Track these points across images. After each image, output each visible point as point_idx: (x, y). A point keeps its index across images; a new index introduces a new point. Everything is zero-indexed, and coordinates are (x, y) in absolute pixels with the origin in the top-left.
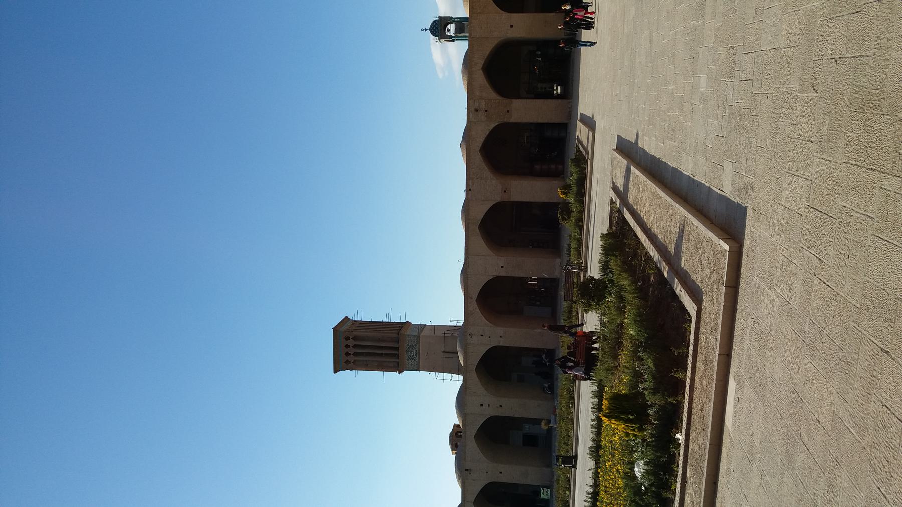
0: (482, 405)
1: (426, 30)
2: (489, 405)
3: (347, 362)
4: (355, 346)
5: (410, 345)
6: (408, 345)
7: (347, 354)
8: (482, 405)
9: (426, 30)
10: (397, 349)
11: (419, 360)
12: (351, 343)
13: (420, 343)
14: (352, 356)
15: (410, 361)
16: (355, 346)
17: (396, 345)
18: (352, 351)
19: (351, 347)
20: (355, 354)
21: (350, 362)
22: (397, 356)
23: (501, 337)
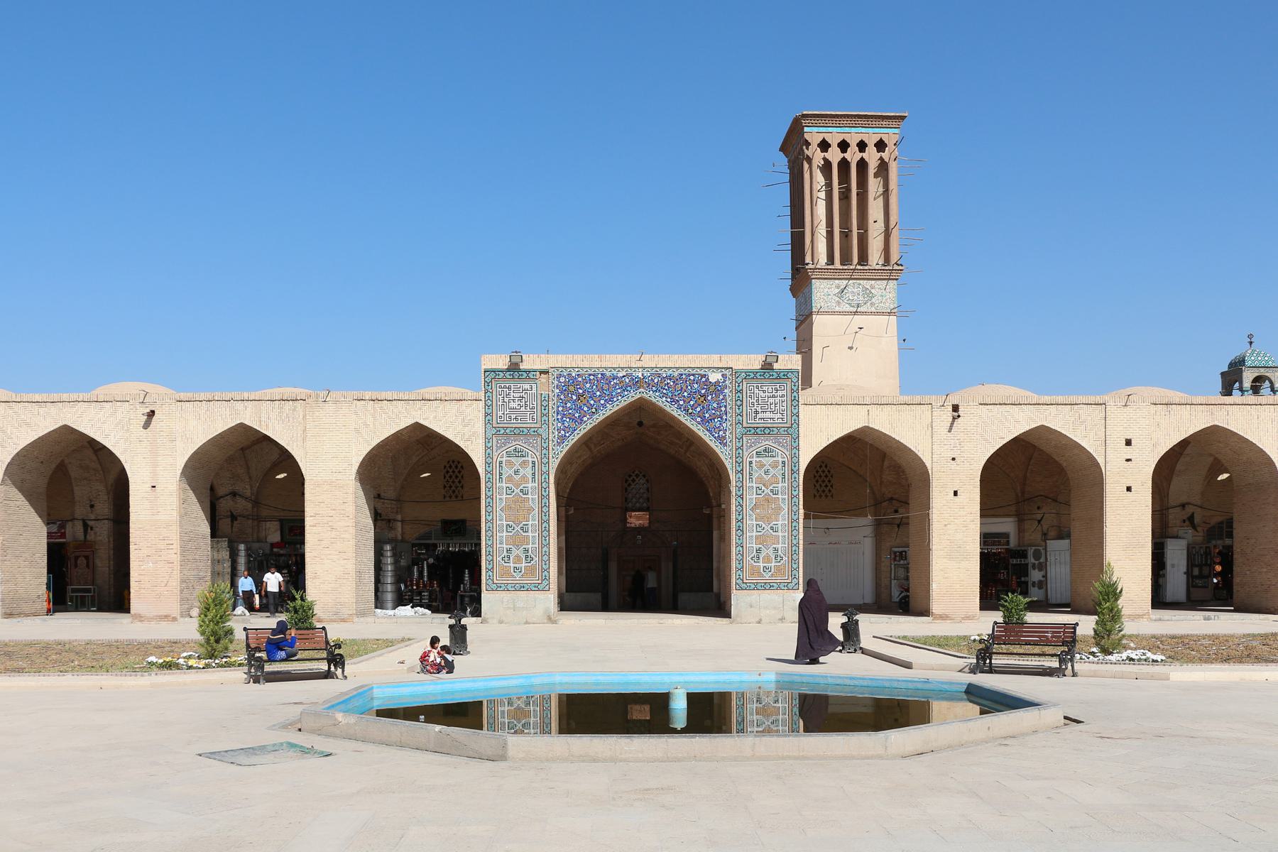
0: (1128, 443)
2: (1128, 460)
5: (873, 291)
7: (844, 146)
8: (1128, 443)
10: (863, 258)
11: (840, 313)
12: (872, 156)
14: (842, 155)
15: (837, 291)
16: (862, 164)
18: (853, 156)
20: (844, 164)
22: (846, 259)
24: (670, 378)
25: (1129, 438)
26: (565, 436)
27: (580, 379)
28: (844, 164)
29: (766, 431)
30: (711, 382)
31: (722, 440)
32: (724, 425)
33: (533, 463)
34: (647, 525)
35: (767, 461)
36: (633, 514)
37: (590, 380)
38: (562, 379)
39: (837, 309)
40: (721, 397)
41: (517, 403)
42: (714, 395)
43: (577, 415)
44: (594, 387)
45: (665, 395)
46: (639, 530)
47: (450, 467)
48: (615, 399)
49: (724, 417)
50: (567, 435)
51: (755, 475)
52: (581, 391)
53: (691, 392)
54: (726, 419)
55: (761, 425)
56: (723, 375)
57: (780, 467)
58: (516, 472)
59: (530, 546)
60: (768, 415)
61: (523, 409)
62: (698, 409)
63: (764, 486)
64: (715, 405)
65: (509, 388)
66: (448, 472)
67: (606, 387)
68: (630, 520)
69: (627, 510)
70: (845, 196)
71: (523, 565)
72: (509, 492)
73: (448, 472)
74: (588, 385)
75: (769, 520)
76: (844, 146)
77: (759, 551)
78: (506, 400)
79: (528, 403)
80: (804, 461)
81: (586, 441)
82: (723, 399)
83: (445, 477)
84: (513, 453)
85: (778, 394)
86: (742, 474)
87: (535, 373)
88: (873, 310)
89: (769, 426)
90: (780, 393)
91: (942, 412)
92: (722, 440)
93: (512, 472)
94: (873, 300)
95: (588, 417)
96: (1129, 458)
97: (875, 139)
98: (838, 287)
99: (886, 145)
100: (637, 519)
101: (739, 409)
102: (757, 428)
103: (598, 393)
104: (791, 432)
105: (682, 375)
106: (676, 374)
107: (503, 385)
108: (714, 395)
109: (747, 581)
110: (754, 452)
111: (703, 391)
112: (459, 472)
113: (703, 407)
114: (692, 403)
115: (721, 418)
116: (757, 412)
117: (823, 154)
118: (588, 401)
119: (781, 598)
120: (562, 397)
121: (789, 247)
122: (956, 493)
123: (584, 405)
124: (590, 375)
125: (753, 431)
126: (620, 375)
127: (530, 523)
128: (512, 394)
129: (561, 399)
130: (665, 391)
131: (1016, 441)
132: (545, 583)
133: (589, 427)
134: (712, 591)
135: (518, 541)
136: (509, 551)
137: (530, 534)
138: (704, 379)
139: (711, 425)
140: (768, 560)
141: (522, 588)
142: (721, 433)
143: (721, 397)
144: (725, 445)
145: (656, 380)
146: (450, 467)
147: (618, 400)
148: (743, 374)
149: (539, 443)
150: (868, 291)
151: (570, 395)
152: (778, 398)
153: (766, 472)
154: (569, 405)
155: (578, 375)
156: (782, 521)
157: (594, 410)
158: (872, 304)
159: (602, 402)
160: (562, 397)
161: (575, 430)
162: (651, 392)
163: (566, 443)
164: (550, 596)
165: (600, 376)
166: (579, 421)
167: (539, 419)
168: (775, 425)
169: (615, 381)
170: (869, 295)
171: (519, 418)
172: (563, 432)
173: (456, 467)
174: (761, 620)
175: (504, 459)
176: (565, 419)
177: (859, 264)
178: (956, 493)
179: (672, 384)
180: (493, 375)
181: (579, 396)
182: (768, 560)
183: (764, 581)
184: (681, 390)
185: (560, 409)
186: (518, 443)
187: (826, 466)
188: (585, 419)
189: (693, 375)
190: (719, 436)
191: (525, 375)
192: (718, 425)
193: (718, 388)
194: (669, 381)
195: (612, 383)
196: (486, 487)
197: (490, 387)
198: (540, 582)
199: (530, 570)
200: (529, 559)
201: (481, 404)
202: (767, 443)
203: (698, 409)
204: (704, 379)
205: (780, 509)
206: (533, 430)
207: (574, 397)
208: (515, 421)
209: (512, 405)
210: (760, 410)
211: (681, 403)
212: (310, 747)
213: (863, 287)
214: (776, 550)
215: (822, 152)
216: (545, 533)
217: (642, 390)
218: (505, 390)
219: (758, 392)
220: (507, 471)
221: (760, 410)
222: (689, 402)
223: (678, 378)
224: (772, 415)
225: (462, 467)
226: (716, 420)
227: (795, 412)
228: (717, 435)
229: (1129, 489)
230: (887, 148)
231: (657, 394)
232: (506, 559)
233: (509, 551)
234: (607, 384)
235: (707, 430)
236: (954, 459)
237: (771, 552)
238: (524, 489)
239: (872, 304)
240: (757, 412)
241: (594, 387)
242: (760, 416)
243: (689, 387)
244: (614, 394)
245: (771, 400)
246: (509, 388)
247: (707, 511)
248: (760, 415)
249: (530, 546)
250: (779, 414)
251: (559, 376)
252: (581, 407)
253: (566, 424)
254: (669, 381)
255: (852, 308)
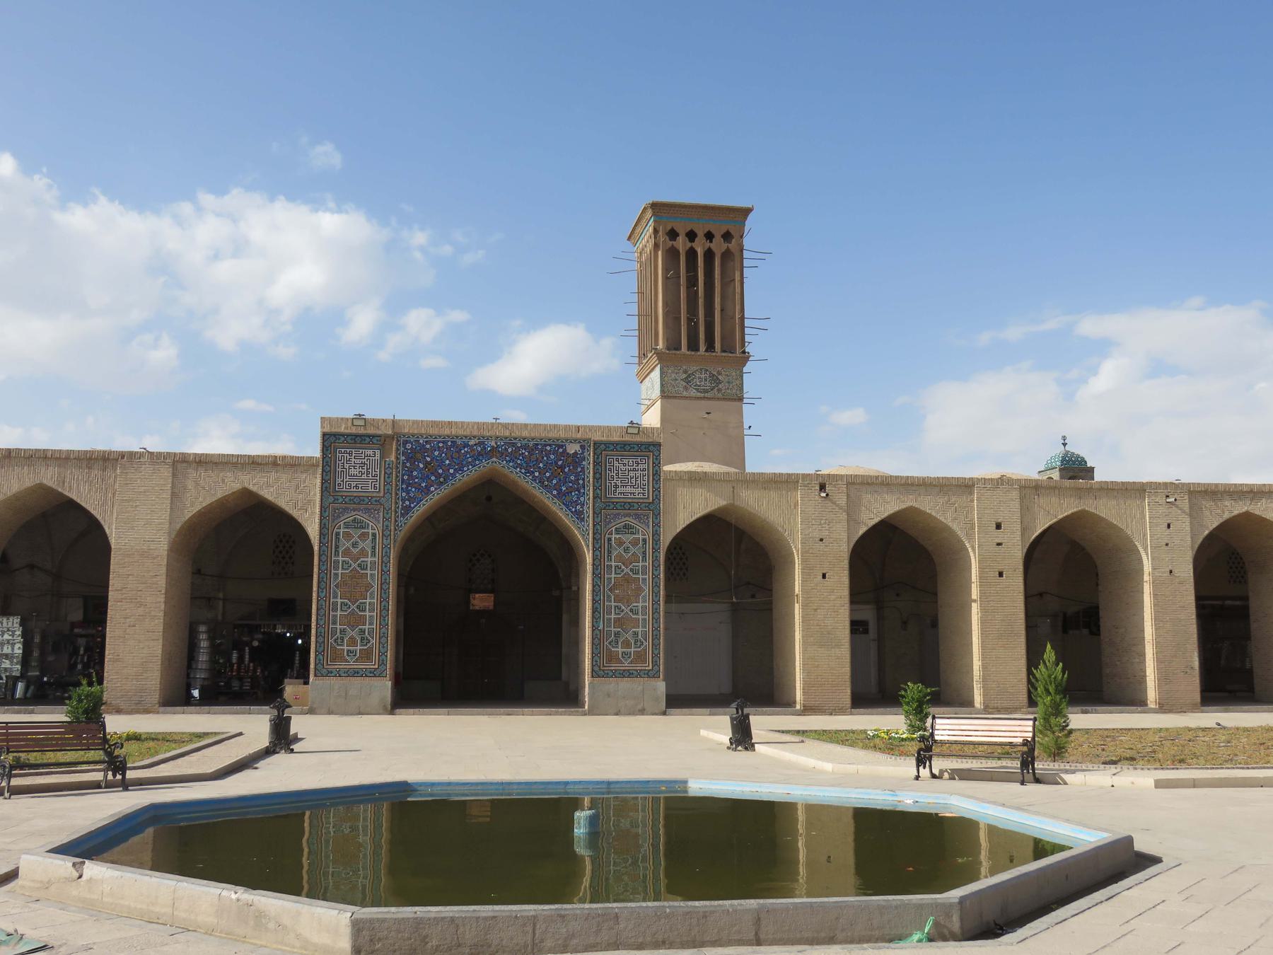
0: (998, 526)
1: (1065, 444)
2: (999, 544)
3: (673, 234)
4: (709, 255)
5: (720, 377)
6: (719, 373)
7: (691, 236)
8: (998, 526)
9: (1065, 444)
10: (710, 347)
11: (686, 398)
12: (718, 246)
13: (724, 399)
14: (689, 245)
15: (684, 376)
16: (709, 255)
17: (718, 345)
19: (708, 244)
20: (692, 254)
21: (675, 241)
22: (693, 346)
23: (1171, 572)
24: (525, 447)
25: (999, 521)
26: (410, 506)
27: (428, 446)
28: (692, 254)
29: (628, 506)
30: (568, 454)
31: (579, 516)
32: (582, 499)
33: (374, 535)
34: (491, 608)
35: (628, 538)
36: (477, 595)
37: (439, 447)
38: (409, 446)
39: (685, 394)
40: (579, 469)
41: (358, 470)
42: (571, 467)
43: (423, 485)
44: (443, 455)
45: (520, 466)
46: (482, 613)
47: (281, 541)
48: (465, 469)
49: (582, 491)
50: (412, 505)
51: (614, 554)
52: (428, 459)
53: (547, 463)
54: (584, 493)
55: (622, 500)
56: (581, 446)
57: (641, 545)
58: (355, 545)
59: (367, 627)
60: (629, 489)
61: (364, 476)
62: (555, 482)
63: (624, 565)
64: (572, 478)
65: (350, 454)
66: (277, 547)
67: (456, 455)
68: (473, 602)
69: (471, 591)
70: (692, 282)
71: (358, 648)
72: (346, 566)
73: (277, 547)
74: (436, 453)
75: (628, 603)
76: (691, 236)
77: (617, 634)
78: (347, 466)
79: (370, 470)
80: (666, 538)
81: (431, 519)
82: (580, 472)
83: (274, 552)
84: (351, 523)
85: (639, 467)
86: (601, 551)
87: (379, 438)
88: (720, 395)
89: (630, 501)
90: (641, 467)
91: (810, 491)
92: (579, 516)
93: (348, 545)
94: (720, 386)
95: (435, 486)
96: (1000, 542)
97: (723, 231)
98: (685, 372)
99: (733, 237)
100: (481, 601)
101: (597, 482)
102: (617, 503)
103: (447, 462)
104: (651, 508)
105: (537, 445)
106: (531, 444)
107: (343, 450)
108: (571, 467)
109: (605, 668)
110: (613, 529)
111: (560, 463)
112: (291, 547)
113: (560, 480)
114: (548, 474)
115: (579, 491)
116: (616, 486)
117: (671, 242)
118: (436, 470)
119: (641, 687)
120: (408, 465)
121: (636, 333)
122: (824, 576)
123: (432, 473)
124: (439, 442)
125: (612, 506)
126: (472, 442)
127: (368, 601)
128: (353, 460)
129: (406, 467)
130: (519, 462)
131: (883, 523)
132: (382, 668)
133: (436, 497)
134: (560, 678)
135: (355, 620)
136: (343, 631)
137: (367, 614)
138: (561, 450)
139: (568, 498)
140: (627, 644)
141: (355, 673)
142: (578, 507)
143: (579, 469)
144: (582, 520)
145: (510, 450)
146: (281, 541)
147: (468, 469)
148: (603, 445)
149: (381, 514)
150: (715, 378)
151: (416, 463)
152: (639, 472)
153: (626, 550)
154: (415, 473)
155: (426, 442)
156: (644, 602)
157: (442, 479)
158: (719, 390)
159: (451, 471)
160: (408, 465)
161: (421, 501)
162: (505, 462)
163: (410, 514)
164: (387, 682)
165: (449, 443)
166: (426, 492)
167: (382, 487)
168: (636, 501)
169: (466, 449)
170: (715, 380)
171: (360, 486)
172: (407, 503)
173: (287, 542)
174: (619, 711)
175: (342, 530)
176: (410, 488)
177: (706, 351)
178: (824, 576)
179: (527, 453)
180: (332, 439)
181: (427, 464)
182: (627, 644)
183: (623, 668)
184: (537, 460)
185: (406, 477)
186: (358, 513)
187: (681, 549)
188: (432, 489)
189: (550, 445)
190: (576, 511)
191: (368, 439)
192: (575, 499)
193: (576, 460)
194: (524, 451)
195: (463, 451)
196: (320, 560)
197: (329, 452)
198: (376, 667)
199: (366, 655)
200: (365, 641)
201: (320, 470)
202: (631, 521)
203: (555, 482)
204: (561, 450)
205: (639, 589)
206: (374, 499)
207: (421, 466)
208: (355, 490)
209: (353, 471)
210: (620, 484)
211: (537, 474)
212: (13, 932)
213: (710, 373)
214: (636, 634)
215: (671, 240)
216: (384, 613)
217: (494, 459)
218: (345, 455)
219: (617, 465)
220: (345, 544)
221: (620, 484)
222: (545, 474)
223: (533, 448)
224: (633, 490)
225: (294, 542)
226: (573, 494)
227: (657, 486)
228: (573, 510)
229: (1001, 574)
230: (734, 240)
231: (511, 464)
232: (339, 640)
233: (343, 631)
234: (457, 452)
235: (564, 504)
236: (821, 540)
237: (629, 636)
238: (363, 564)
239: (719, 390)
240: (616, 486)
241: (443, 455)
242: (619, 490)
243: (545, 458)
244: (465, 462)
245: (632, 474)
246: (350, 454)
247: (556, 593)
248: (620, 489)
249: (367, 627)
250: (639, 489)
251: (406, 442)
252: (428, 476)
253: (412, 495)
254: (524, 451)
255: (699, 394)
